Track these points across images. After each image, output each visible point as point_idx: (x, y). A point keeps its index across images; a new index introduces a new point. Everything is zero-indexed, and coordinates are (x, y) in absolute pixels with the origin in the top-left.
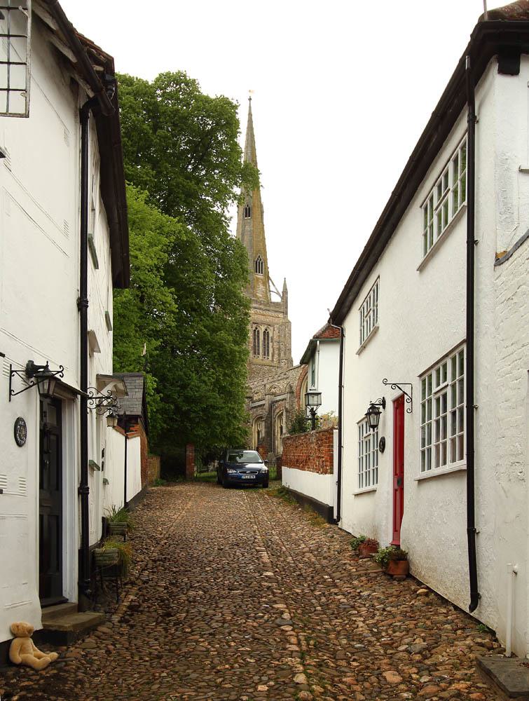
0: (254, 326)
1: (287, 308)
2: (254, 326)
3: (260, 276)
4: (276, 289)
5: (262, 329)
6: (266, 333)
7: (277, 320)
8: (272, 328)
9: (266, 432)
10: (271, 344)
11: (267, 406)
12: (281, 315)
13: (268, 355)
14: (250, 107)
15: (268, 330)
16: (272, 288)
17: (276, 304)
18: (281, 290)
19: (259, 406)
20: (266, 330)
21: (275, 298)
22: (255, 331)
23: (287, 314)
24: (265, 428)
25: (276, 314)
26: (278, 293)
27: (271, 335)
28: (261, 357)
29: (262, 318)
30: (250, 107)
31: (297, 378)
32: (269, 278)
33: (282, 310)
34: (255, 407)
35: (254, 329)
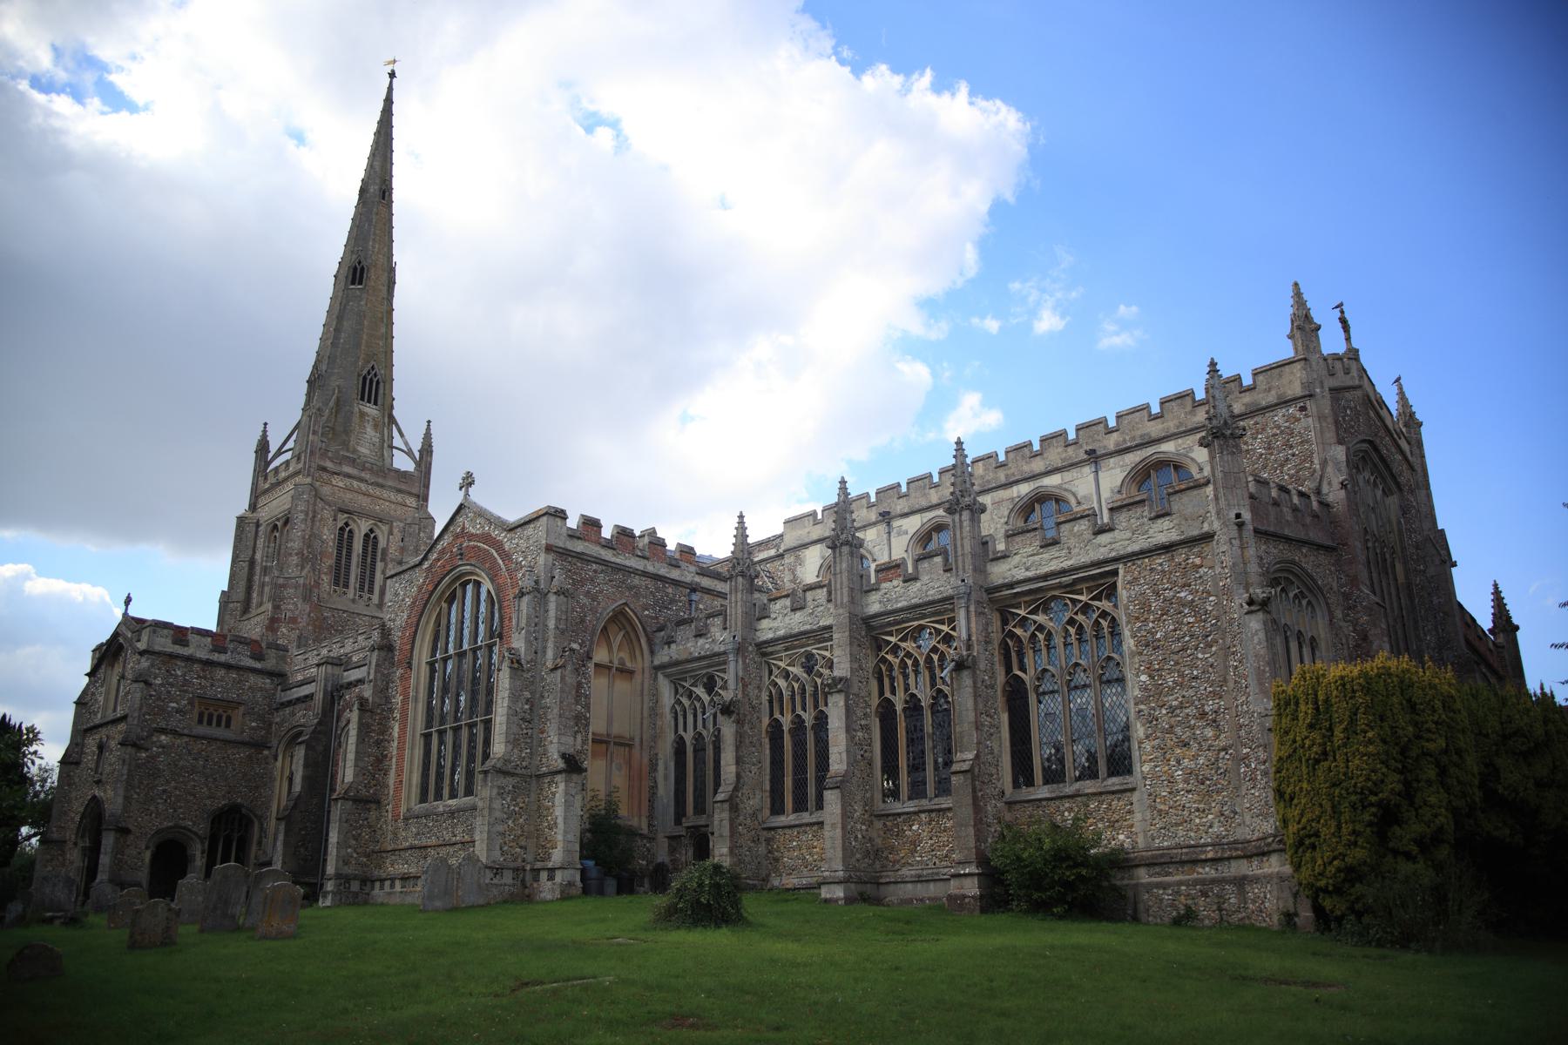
0: (342, 518)
1: (427, 486)
2: (342, 518)
3: (371, 410)
4: (406, 444)
5: (361, 527)
6: (370, 539)
7: (400, 511)
8: (385, 528)
9: (305, 778)
10: (379, 566)
11: (319, 697)
12: (411, 502)
13: (371, 591)
14: (389, 101)
15: (378, 532)
16: (398, 441)
17: (403, 475)
18: (416, 447)
19: (299, 700)
20: (372, 531)
21: (403, 463)
22: (342, 529)
23: (426, 499)
24: (306, 766)
25: (399, 497)
26: (409, 453)
27: (382, 543)
28: (351, 595)
29: (364, 502)
30: (389, 101)
31: (408, 601)
32: (392, 420)
33: (415, 491)
34: (290, 703)
35: (340, 524)
